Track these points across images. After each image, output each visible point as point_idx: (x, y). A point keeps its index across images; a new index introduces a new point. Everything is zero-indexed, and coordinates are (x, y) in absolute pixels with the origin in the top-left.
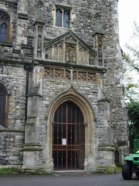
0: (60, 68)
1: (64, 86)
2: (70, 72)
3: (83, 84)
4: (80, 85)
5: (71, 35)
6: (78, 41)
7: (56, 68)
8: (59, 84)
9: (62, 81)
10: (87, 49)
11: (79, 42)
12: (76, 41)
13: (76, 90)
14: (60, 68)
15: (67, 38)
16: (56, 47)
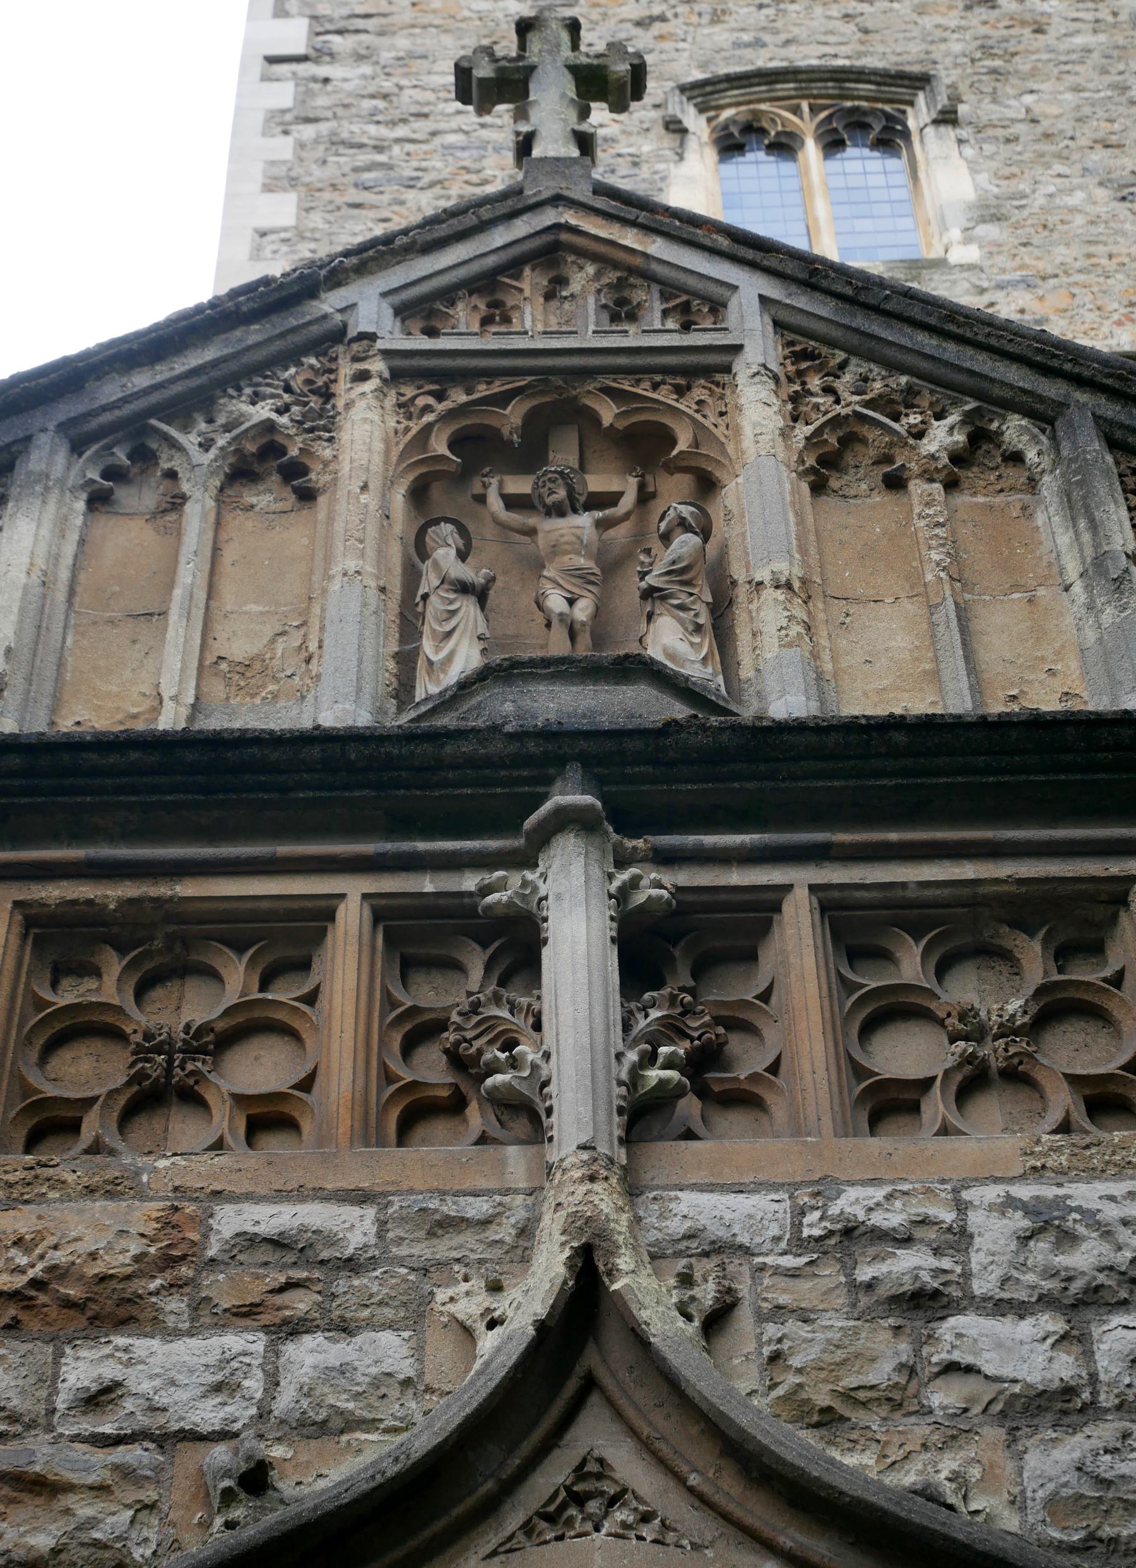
0: (187, 889)
1: (308, 1355)
2: (517, 945)
3: (1049, 1224)
4: (909, 1265)
5: (570, 217)
6: (749, 288)
7: (53, 893)
8: (108, 1308)
9: (229, 1221)
10: (1052, 389)
11: (802, 301)
12: (694, 304)
13: (799, 1445)
14: (187, 889)
15: (449, 294)
16: (143, 497)
